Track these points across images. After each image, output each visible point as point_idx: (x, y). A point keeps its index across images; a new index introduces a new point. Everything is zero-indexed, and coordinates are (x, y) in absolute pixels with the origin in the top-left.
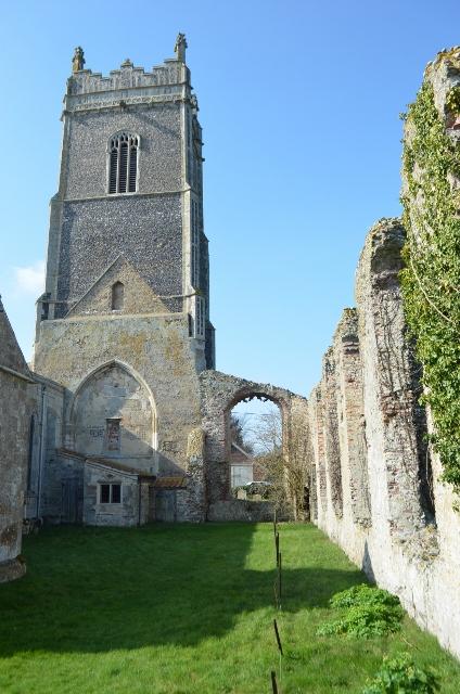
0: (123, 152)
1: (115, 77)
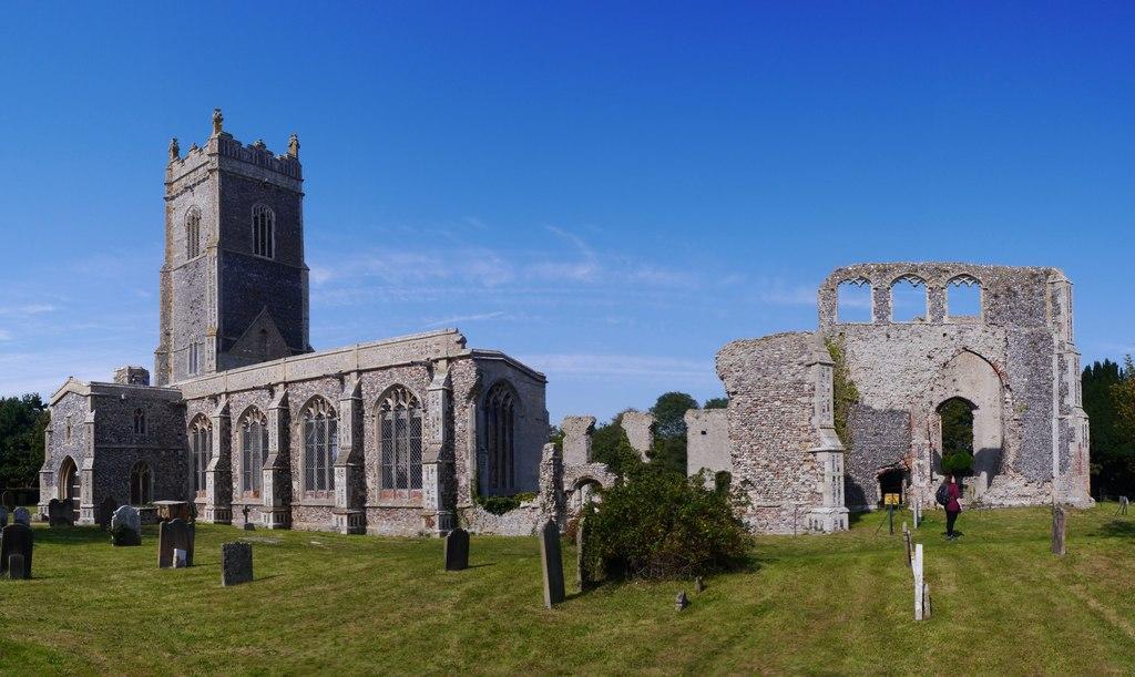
0: (263, 221)
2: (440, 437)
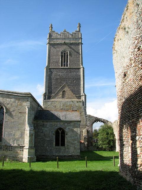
0: (65, 56)
1: (62, 34)
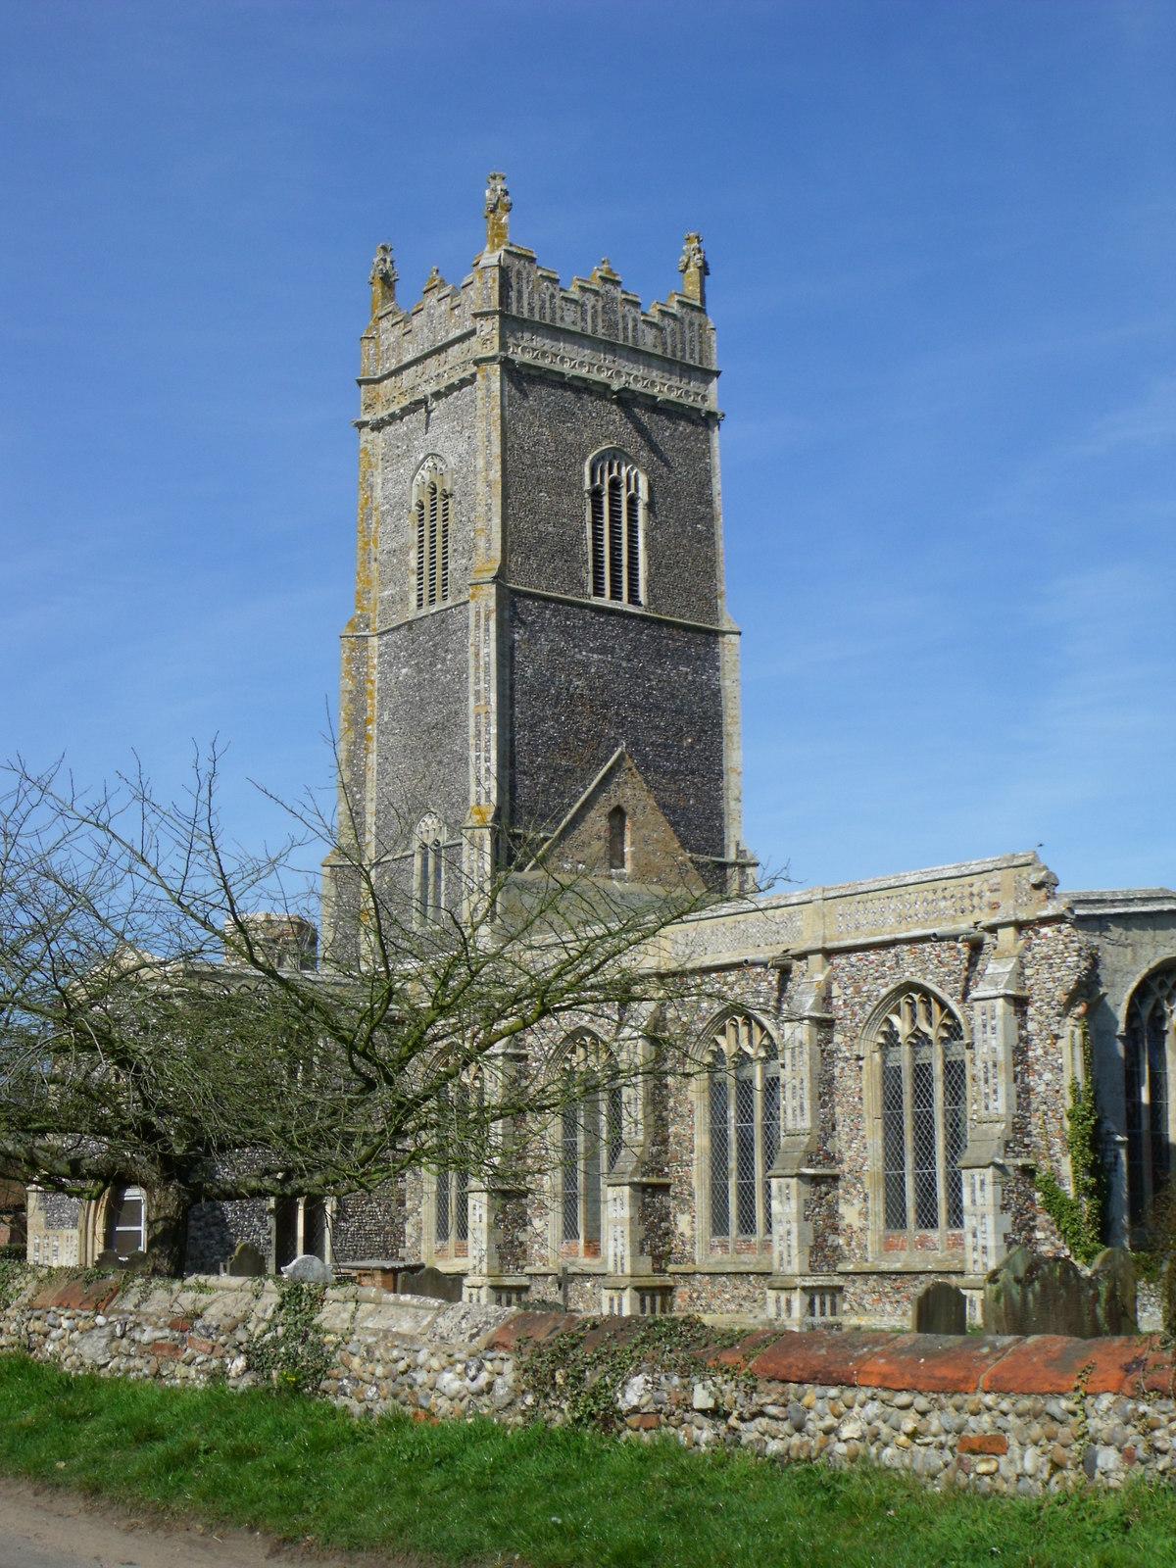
0: (614, 502)
1: (590, 300)
2: (1000, 1105)
